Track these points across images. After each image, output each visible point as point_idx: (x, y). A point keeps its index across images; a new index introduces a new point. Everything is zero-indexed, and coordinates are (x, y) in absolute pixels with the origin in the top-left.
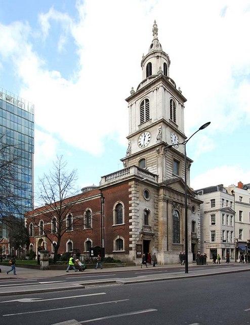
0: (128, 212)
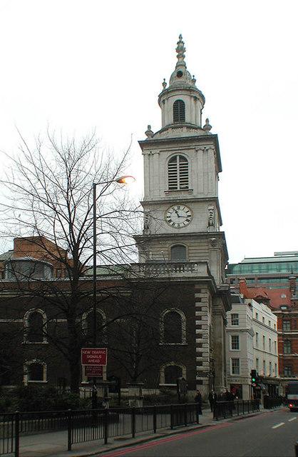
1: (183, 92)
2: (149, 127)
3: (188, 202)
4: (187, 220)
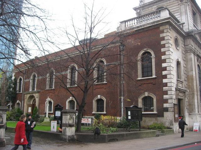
0: (160, 61)
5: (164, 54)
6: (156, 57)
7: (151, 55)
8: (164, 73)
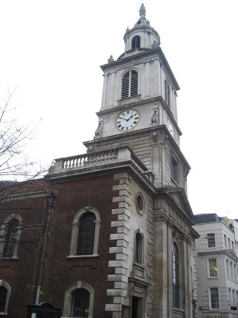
0: (108, 230)
1: (141, 30)
2: (111, 56)
3: (136, 106)
4: (135, 123)
5: (115, 218)
6: (101, 223)
7: (95, 219)
8: (112, 250)
